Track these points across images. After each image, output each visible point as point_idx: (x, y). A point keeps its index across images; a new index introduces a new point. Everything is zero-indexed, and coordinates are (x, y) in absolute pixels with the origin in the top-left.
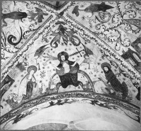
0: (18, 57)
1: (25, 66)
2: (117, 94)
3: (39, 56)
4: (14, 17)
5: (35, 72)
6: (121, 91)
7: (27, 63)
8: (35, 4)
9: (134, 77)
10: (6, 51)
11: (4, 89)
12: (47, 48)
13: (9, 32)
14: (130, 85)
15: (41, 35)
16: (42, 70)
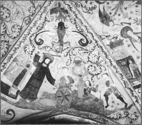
0: (97, 45)
1: (118, 39)
3: (111, 21)
4: (63, 33)
5: (132, 30)
7: (115, 36)
8: (42, 16)
10: (92, 51)
11: (133, 70)
12: (104, 8)
13: (76, 43)
15: (78, 16)
16: (132, 21)
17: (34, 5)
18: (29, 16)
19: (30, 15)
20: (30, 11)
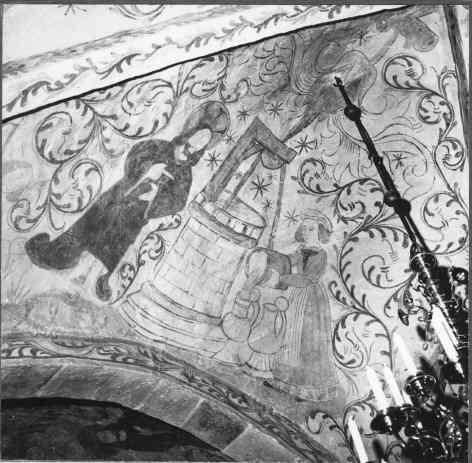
17: (422, 88)
18: (441, 136)
19: (441, 130)
20: (428, 117)
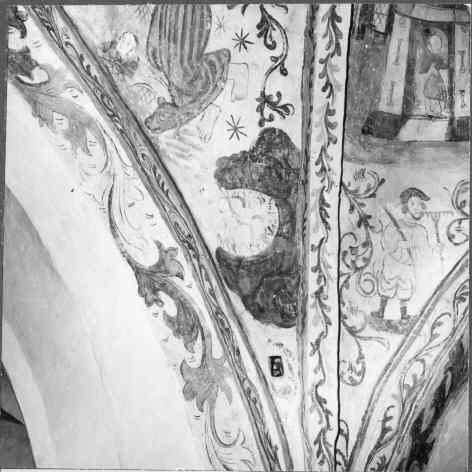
2: (137, 78)
6: (170, 83)
9: (321, 62)
14: (238, 92)
